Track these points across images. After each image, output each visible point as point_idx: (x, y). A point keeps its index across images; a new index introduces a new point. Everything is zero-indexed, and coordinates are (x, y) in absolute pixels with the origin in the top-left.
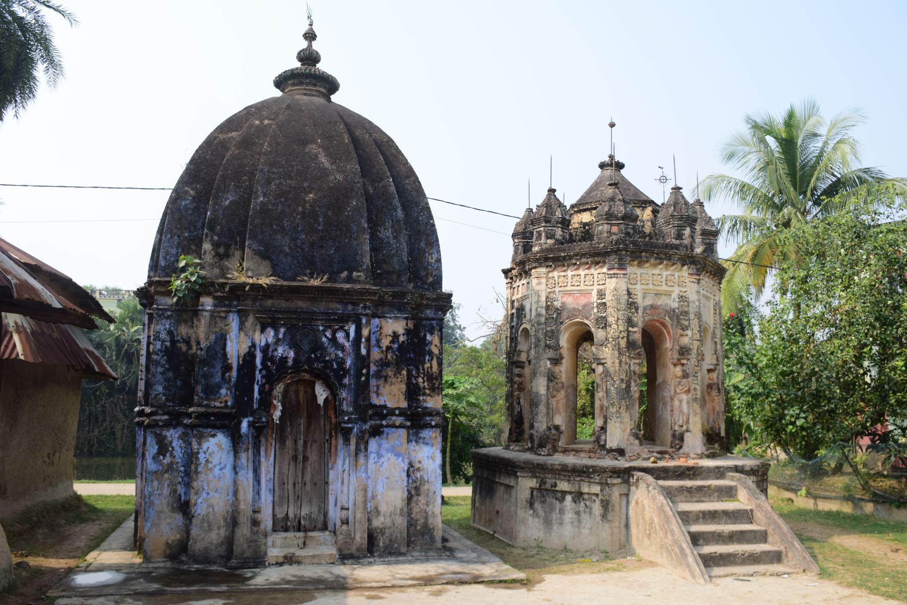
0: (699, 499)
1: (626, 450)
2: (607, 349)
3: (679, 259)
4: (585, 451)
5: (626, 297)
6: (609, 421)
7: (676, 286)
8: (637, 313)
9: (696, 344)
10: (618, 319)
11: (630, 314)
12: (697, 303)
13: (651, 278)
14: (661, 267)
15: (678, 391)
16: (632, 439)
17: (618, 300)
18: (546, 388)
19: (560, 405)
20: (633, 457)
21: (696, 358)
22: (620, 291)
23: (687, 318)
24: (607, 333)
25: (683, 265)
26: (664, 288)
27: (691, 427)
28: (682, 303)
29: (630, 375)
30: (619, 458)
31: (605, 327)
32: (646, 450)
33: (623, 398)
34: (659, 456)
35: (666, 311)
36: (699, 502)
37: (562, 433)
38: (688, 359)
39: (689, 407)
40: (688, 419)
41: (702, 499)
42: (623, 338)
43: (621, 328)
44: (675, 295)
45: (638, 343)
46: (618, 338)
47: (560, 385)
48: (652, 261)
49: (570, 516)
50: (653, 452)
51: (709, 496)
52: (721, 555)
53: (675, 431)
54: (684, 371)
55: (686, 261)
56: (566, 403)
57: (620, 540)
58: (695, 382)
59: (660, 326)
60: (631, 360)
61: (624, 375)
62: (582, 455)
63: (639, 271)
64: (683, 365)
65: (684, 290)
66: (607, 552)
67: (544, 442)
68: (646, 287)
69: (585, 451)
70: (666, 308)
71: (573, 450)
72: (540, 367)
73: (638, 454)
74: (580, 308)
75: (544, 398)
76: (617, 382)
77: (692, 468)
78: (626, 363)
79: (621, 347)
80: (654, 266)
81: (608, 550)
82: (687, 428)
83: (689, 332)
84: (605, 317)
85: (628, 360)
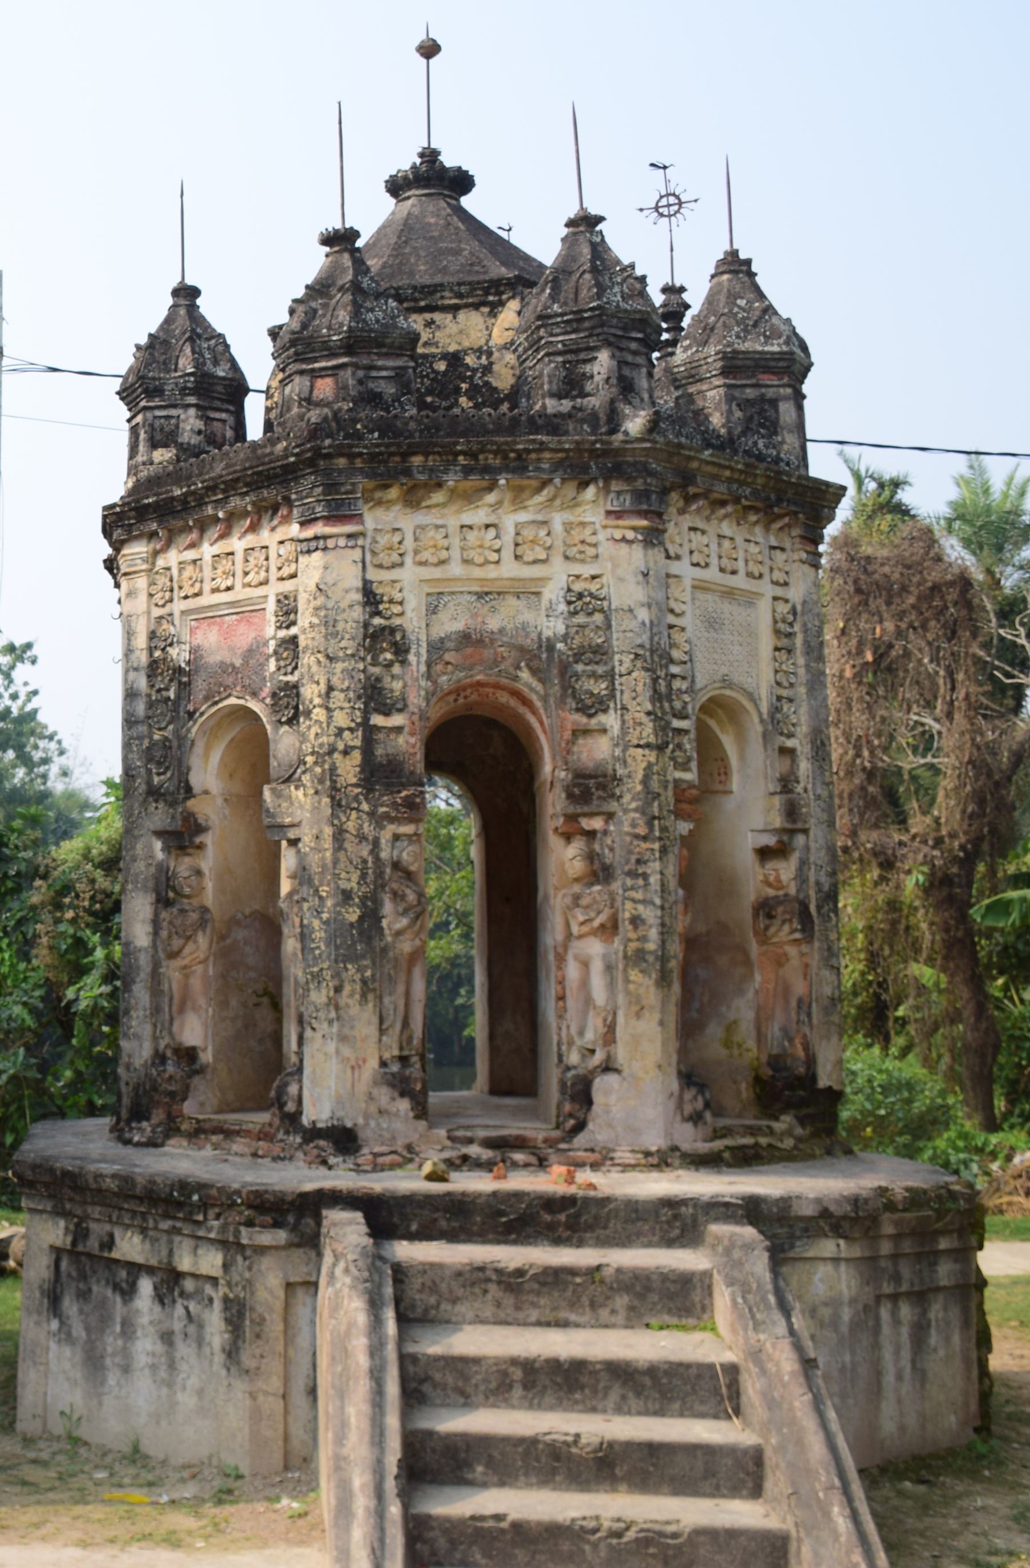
0: (549, 1316)
1: (361, 1135)
2: (300, 793)
3: (557, 466)
4: (247, 1133)
5: (358, 613)
6: (308, 1033)
7: (557, 560)
8: (404, 662)
9: (640, 760)
10: (330, 689)
11: (376, 670)
12: (643, 615)
13: (455, 541)
14: (491, 498)
15: (575, 929)
16: (384, 1095)
17: (329, 625)
18: (149, 928)
19: (196, 983)
20: (387, 1159)
21: (642, 811)
22: (336, 594)
23: (600, 670)
24: (303, 738)
25: (583, 485)
26: (509, 569)
27: (622, 1054)
28: (581, 619)
29: (379, 874)
30: (332, 1160)
31: (292, 721)
32: (442, 1133)
33: (351, 957)
34: (486, 1154)
35: (522, 649)
36: (548, 1324)
37: (201, 1071)
38: (610, 816)
39: (611, 985)
40: (611, 1029)
41: (564, 1314)
42: (346, 752)
43: (341, 719)
44: (553, 592)
45: (407, 768)
46: (332, 750)
47: (194, 916)
48: (451, 480)
49: (149, 1347)
50: (470, 1141)
51: (593, 1305)
52: (518, 1527)
53: (568, 1068)
54: (591, 857)
55: (586, 469)
56: (224, 976)
57: (286, 1438)
58: (639, 895)
59: (513, 702)
60: (379, 826)
61: (355, 877)
62: (235, 1147)
63: (408, 521)
64: (591, 834)
65: (587, 570)
66: (239, 1477)
67: (144, 1101)
68: (437, 573)
69: (247, 1133)
70: (520, 641)
71: (218, 1130)
72: (134, 859)
73: (409, 1148)
74: (238, 663)
75: (144, 961)
76: (329, 903)
77: (567, 1202)
78: (362, 838)
79: (341, 782)
80: (470, 498)
81: (244, 1470)
82: (609, 1058)
83: (611, 720)
84: (296, 686)
85: (367, 828)
